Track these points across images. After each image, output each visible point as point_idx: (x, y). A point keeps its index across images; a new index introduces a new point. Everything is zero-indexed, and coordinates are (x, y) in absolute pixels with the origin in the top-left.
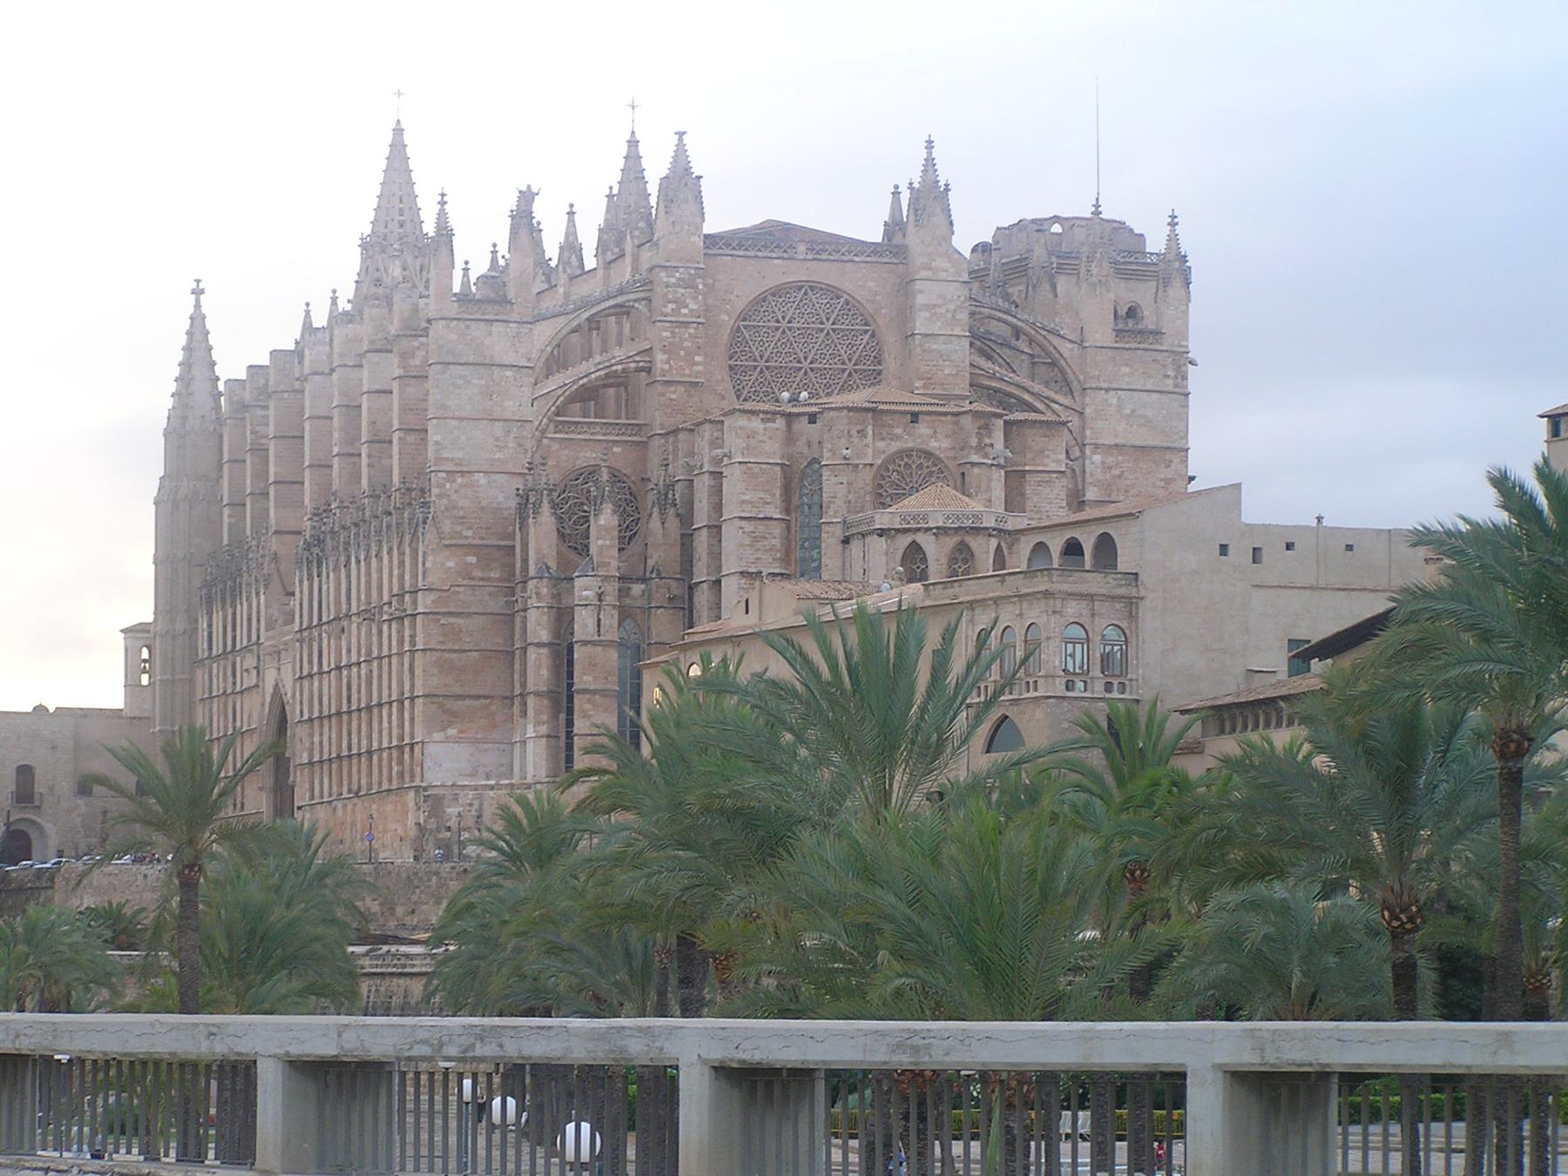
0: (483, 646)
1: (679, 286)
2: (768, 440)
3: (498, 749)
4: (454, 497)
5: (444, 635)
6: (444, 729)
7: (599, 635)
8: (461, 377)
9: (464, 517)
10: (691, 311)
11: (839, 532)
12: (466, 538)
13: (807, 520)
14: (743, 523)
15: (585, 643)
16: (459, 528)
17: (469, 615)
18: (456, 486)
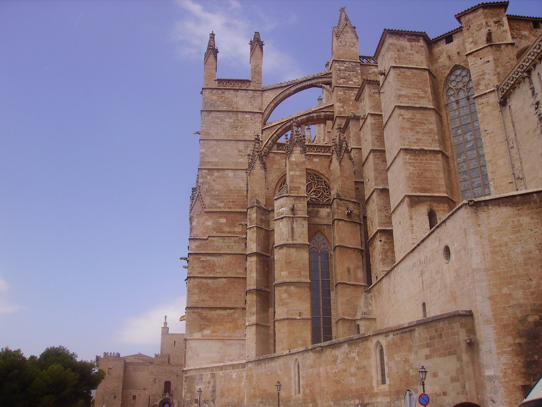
0: (229, 275)
1: (346, 70)
2: (415, 53)
3: (240, 344)
4: (213, 184)
5: (203, 267)
6: (201, 330)
7: (293, 240)
8: (218, 118)
9: (218, 195)
10: (355, 82)
11: (494, 99)
12: (220, 208)
13: (457, 113)
14: (402, 112)
15: (281, 246)
16: (215, 202)
17: (220, 255)
18: (213, 177)
